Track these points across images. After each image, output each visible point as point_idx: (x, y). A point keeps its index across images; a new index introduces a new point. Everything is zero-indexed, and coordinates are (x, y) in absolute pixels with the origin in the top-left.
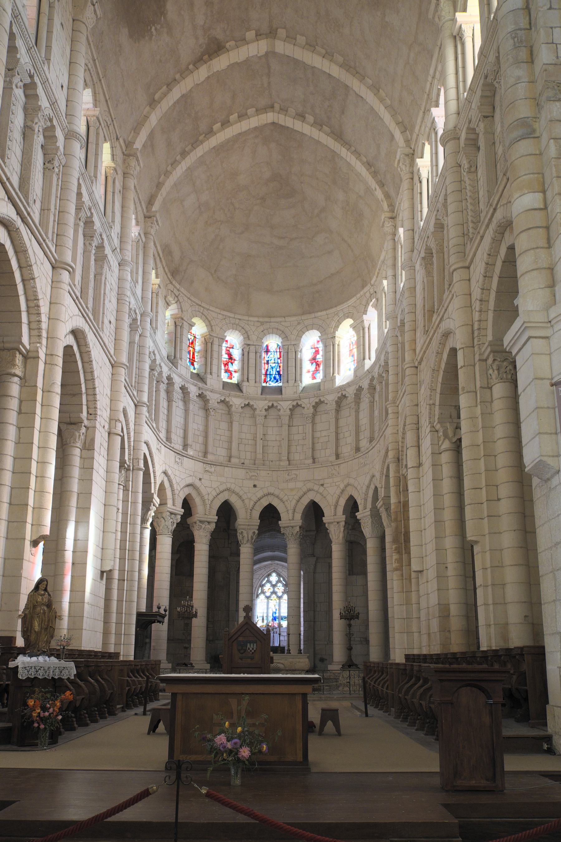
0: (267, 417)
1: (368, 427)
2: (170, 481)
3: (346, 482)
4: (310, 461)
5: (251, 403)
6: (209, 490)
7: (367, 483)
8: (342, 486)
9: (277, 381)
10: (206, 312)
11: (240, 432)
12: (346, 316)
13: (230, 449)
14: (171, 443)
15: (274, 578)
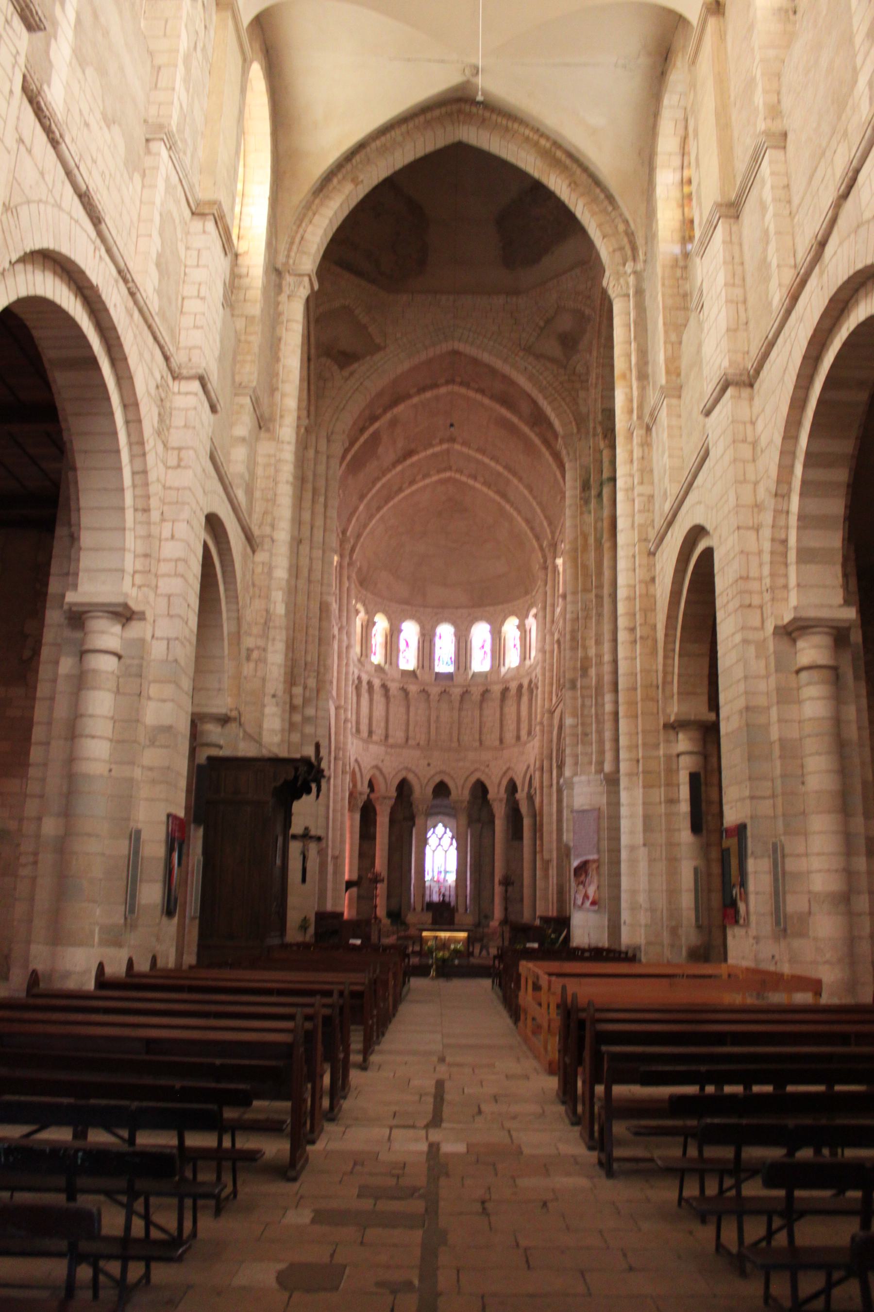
3: (507, 766)
4: (477, 744)
5: (426, 688)
8: (504, 768)
15: (440, 828)
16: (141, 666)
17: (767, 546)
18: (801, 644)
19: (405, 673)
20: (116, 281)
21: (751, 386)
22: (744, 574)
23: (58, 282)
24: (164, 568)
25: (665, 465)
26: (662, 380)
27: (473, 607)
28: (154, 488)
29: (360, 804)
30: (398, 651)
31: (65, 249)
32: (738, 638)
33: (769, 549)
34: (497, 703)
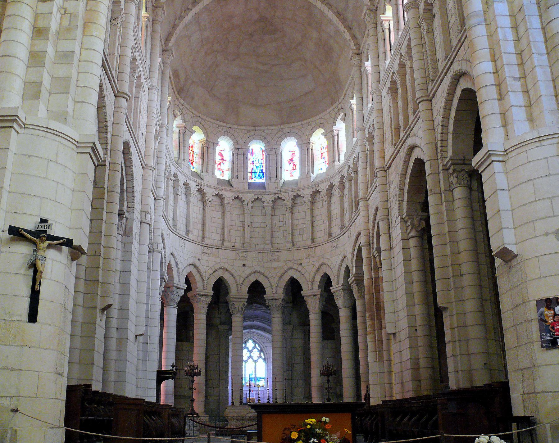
0: (253, 208)
1: (339, 216)
2: (176, 261)
3: (320, 263)
5: (240, 197)
6: (207, 268)
7: (339, 262)
8: (317, 265)
9: (261, 178)
12: (320, 126)
13: (223, 234)
14: (176, 229)
15: (250, 344)
19: (220, 182)
27: (283, 123)
29: (178, 299)
30: (214, 162)
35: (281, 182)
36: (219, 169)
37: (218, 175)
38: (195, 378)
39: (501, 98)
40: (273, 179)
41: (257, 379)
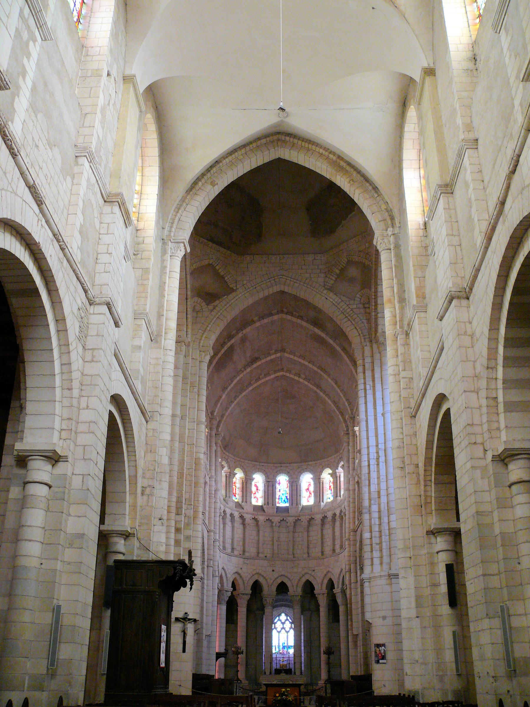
2: (225, 572)
4: (306, 555)
8: (325, 572)
9: (286, 503)
10: (243, 464)
11: (264, 536)
15: (283, 617)
16: (64, 493)
17: (484, 402)
18: (511, 467)
19: (256, 508)
20: (52, 241)
21: (468, 298)
22: (470, 422)
23: (13, 239)
24: (82, 427)
25: (419, 356)
26: (414, 301)
27: (301, 462)
28: (76, 375)
29: (227, 599)
30: (251, 492)
31: (18, 219)
32: (469, 465)
33: (485, 405)
34: (319, 526)
35: (300, 507)
36: (255, 497)
37: (254, 502)
38: (239, 656)
39: (372, 551)
40: (294, 505)
41: (289, 647)
